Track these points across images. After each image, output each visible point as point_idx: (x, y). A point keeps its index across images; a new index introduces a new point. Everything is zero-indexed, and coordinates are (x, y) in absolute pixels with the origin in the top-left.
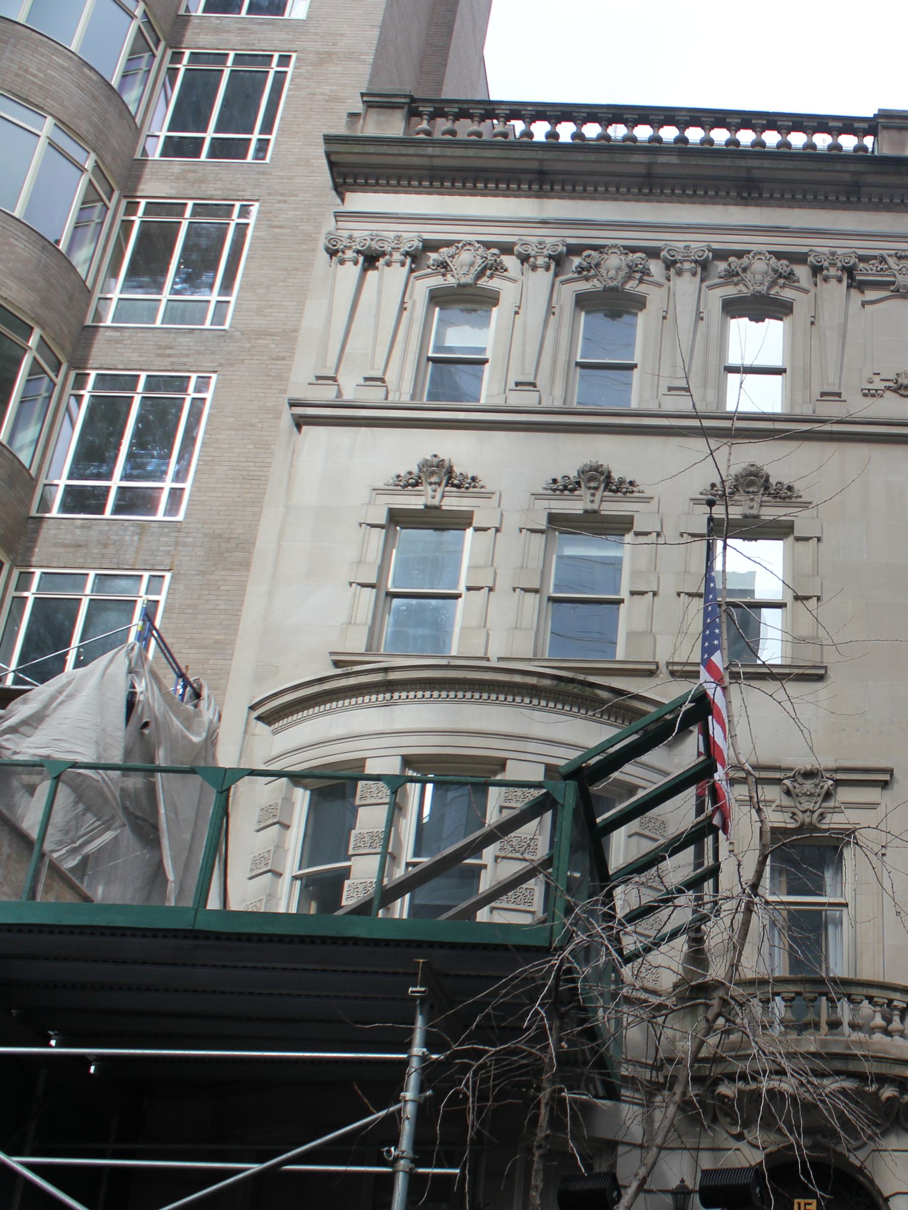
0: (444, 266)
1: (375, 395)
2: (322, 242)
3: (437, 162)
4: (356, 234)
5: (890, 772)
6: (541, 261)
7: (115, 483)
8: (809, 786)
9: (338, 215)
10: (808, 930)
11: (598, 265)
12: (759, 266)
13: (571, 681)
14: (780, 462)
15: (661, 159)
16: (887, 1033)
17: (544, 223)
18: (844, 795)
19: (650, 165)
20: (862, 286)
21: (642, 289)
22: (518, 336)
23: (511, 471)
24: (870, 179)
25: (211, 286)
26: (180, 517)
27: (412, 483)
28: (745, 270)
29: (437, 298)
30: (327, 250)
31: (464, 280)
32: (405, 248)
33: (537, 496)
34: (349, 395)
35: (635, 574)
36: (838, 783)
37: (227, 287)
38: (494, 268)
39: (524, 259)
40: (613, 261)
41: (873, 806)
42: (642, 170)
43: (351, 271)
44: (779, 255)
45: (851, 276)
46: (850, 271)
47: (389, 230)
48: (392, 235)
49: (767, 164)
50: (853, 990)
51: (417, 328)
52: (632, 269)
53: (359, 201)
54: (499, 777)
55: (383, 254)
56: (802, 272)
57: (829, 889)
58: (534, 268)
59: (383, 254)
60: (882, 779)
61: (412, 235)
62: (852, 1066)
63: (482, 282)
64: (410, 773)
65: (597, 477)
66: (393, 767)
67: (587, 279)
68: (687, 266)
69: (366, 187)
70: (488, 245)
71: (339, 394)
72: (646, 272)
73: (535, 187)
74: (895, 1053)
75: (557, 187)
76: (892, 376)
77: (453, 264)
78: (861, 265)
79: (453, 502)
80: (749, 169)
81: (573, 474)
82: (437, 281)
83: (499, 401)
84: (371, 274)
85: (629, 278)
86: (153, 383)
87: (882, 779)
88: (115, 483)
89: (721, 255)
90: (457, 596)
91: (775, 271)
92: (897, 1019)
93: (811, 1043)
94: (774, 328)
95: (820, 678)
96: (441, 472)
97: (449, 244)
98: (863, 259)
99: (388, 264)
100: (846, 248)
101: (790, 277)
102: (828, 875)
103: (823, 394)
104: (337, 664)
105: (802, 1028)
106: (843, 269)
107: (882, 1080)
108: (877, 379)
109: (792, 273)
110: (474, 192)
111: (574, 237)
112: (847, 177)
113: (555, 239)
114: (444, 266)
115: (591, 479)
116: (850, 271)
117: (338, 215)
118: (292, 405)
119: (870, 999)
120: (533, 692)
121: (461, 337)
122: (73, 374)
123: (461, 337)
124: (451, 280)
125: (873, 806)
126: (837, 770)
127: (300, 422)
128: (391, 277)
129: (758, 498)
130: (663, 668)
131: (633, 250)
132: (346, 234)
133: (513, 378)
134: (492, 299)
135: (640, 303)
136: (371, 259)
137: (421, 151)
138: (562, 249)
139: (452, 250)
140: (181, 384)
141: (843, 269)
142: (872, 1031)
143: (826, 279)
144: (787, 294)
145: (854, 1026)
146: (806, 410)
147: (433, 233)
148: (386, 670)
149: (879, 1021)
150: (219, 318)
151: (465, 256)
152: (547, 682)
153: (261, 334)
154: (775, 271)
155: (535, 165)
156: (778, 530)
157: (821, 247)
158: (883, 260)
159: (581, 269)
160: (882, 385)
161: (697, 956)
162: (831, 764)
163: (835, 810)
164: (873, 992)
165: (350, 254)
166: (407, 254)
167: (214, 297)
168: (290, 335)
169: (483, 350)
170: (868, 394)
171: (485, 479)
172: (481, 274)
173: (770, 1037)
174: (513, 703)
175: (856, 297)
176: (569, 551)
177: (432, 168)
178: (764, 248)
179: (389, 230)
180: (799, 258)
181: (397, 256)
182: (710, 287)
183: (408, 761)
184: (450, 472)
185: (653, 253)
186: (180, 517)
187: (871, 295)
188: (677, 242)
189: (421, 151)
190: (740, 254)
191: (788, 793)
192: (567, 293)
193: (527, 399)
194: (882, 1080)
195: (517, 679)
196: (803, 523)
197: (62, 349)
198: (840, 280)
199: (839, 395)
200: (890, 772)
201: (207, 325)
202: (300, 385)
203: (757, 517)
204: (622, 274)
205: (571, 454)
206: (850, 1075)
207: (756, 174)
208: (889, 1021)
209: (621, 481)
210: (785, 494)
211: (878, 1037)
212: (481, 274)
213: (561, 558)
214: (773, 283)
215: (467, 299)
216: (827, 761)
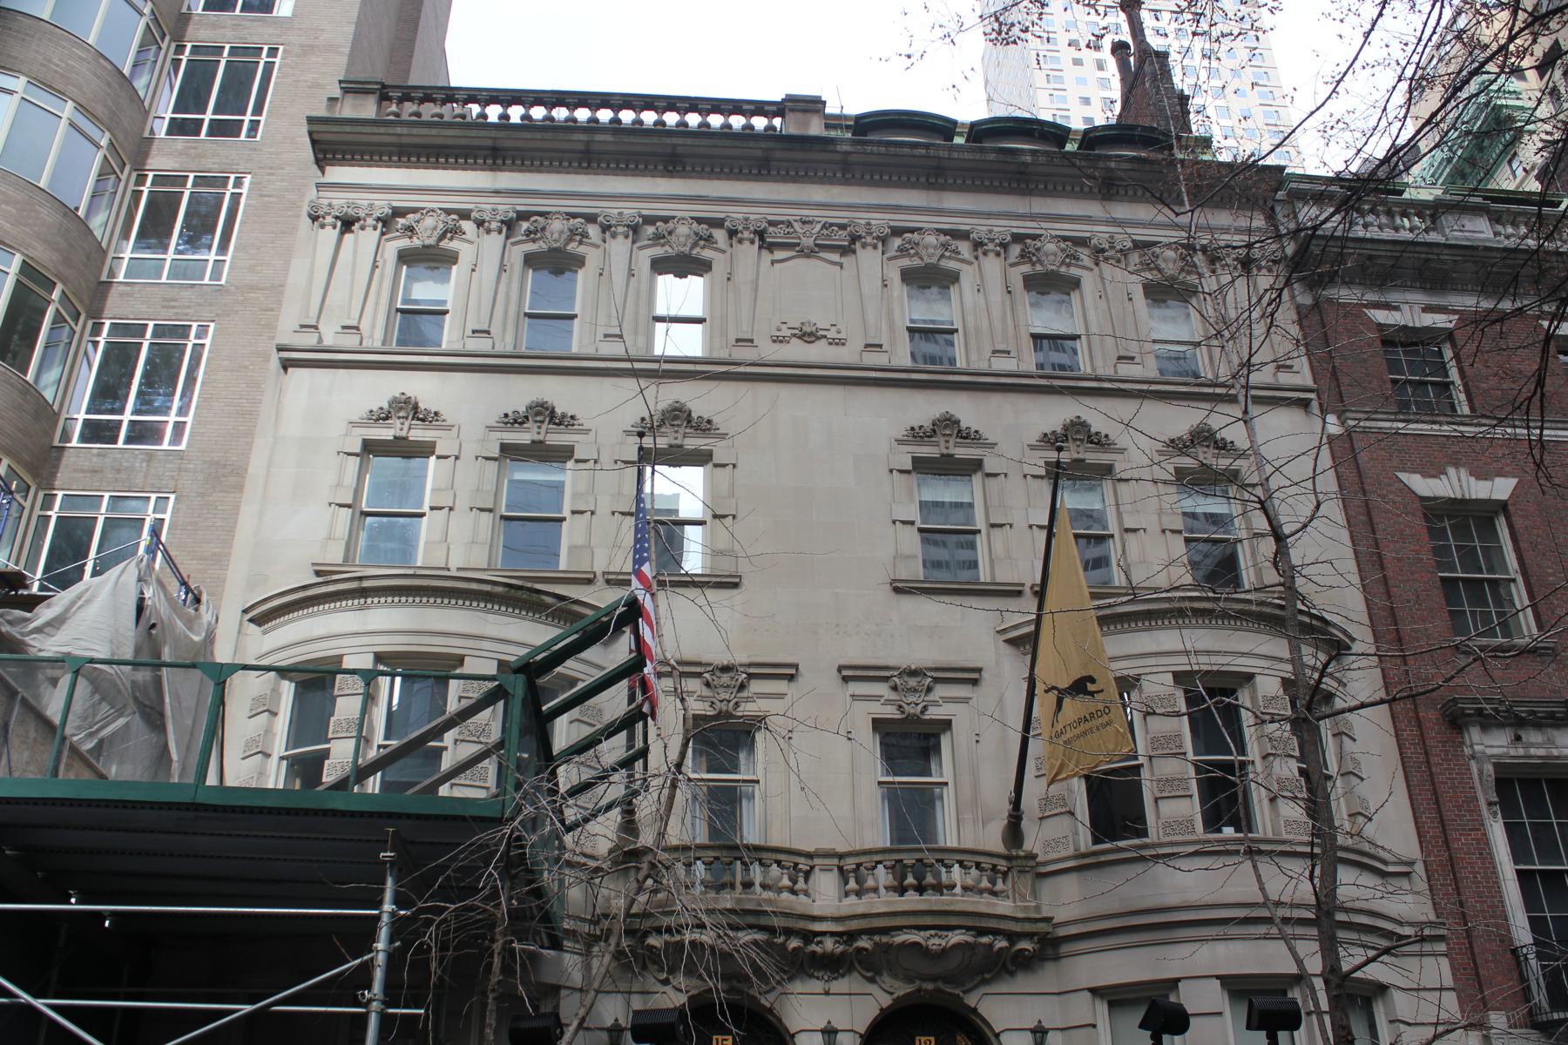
0: (410, 230)
1: (350, 341)
2: (306, 209)
3: (405, 140)
4: (335, 202)
5: (796, 666)
6: (494, 225)
7: (127, 417)
8: (725, 678)
9: (319, 186)
10: (725, 804)
11: (543, 229)
12: (683, 230)
13: (521, 588)
14: (700, 399)
15: (599, 137)
16: (793, 892)
17: (497, 192)
18: (756, 686)
19: (588, 143)
20: (771, 247)
21: (582, 249)
22: (475, 290)
23: (468, 407)
24: (779, 154)
25: (210, 247)
26: (183, 447)
27: (383, 417)
28: (670, 233)
29: (405, 257)
30: (310, 216)
31: (427, 242)
32: (377, 214)
33: (491, 428)
34: (328, 341)
35: (575, 495)
36: (751, 676)
37: (223, 248)
38: (455, 232)
39: (480, 224)
40: (557, 225)
41: (781, 696)
42: (581, 147)
43: (330, 234)
44: (700, 221)
45: (762, 239)
46: (761, 234)
47: (363, 199)
48: (366, 203)
49: (689, 141)
50: (764, 855)
51: (387, 284)
52: (573, 232)
53: (337, 174)
54: (458, 671)
55: (358, 219)
56: (720, 235)
57: (743, 768)
58: (488, 231)
59: (358, 219)
60: (788, 673)
61: (383, 203)
62: (763, 921)
63: (443, 244)
64: (381, 668)
65: (543, 412)
66: (366, 662)
67: (534, 241)
68: (620, 229)
69: (343, 162)
70: (448, 212)
71: (320, 340)
72: (585, 235)
73: (489, 161)
74: (800, 910)
75: (508, 162)
76: (797, 325)
77: (419, 228)
78: (771, 229)
79: (418, 434)
80: (674, 146)
81: (522, 409)
82: (404, 243)
83: (458, 347)
84: (347, 236)
85: (571, 240)
86: (159, 331)
87: (788, 673)
88: (127, 417)
89: (650, 220)
90: (422, 515)
91: (696, 234)
92: (801, 880)
93: (727, 900)
94: (695, 284)
95: (735, 586)
96: (408, 408)
97: (414, 210)
98: (772, 223)
99: (363, 228)
100: (757, 214)
101: (709, 239)
102: (742, 756)
103: (738, 340)
104: (318, 573)
105: (720, 888)
106: (755, 232)
107: (789, 932)
108: (784, 327)
109: (711, 236)
110: (436, 166)
111: (523, 204)
112: (759, 153)
113: (506, 207)
114: (410, 230)
115: (538, 414)
116: (761, 234)
117: (319, 186)
118: (280, 349)
119: (779, 863)
120: (488, 597)
121: (426, 291)
122: (90, 323)
123: (426, 291)
124: (416, 242)
125: (781, 696)
126: (750, 665)
127: (286, 365)
128: (365, 240)
129: (682, 430)
130: (600, 577)
131: (574, 216)
132: (326, 202)
133: (470, 326)
134: (452, 258)
135: (580, 261)
136: (347, 224)
137: (391, 131)
138: (512, 215)
139: (418, 216)
140: (183, 331)
141: (755, 232)
142: (780, 890)
143: (740, 241)
144: (707, 254)
145: (764, 886)
146: (723, 354)
147: (401, 201)
148: (360, 579)
149: (786, 882)
150: (216, 274)
151: (429, 222)
152: (499, 589)
153: (253, 288)
154: (696, 234)
155: (489, 143)
156: (700, 458)
157: (736, 213)
158: (789, 224)
159: (528, 233)
161: (629, 826)
162: (745, 660)
163: (748, 700)
164: (781, 857)
165: (329, 219)
166: (378, 219)
167: (212, 256)
168: (278, 289)
169: (444, 302)
170: (777, 340)
171: (445, 414)
172: (442, 237)
173: (692, 895)
175: (767, 257)
176: (518, 476)
177: (401, 145)
178: (687, 214)
179: (363, 199)
180: (717, 223)
181: (370, 221)
182: (641, 248)
183: (379, 658)
184: (416, 407)
185: (591, 219)
186: (183, 447)
187: (779, 255)
188: (612, 209)
189: (391, 131)
190: (666, 220)
191: (708, 685)
192: (517, 254)
193: (482, 344)
194: (789, 932)
195: (474, 586)
196: (721, 453)
197: (81, 301)
198: (752, 242)
199: (751, 341)
200: (796, 666)
201: (206, 281)
202: (287, 333)
203: (681, 446)
204: (564, 236)
205: (520, 392)
206: (761, 928)
207: (680, 150)
208: (795, 882)
209: (564, 416)
210: (704, 427)
211: (785, 895)
212: (442, 237)
213: (510, 481)
214: (695, 245)
215: (433, 258)
216: (741, 657)
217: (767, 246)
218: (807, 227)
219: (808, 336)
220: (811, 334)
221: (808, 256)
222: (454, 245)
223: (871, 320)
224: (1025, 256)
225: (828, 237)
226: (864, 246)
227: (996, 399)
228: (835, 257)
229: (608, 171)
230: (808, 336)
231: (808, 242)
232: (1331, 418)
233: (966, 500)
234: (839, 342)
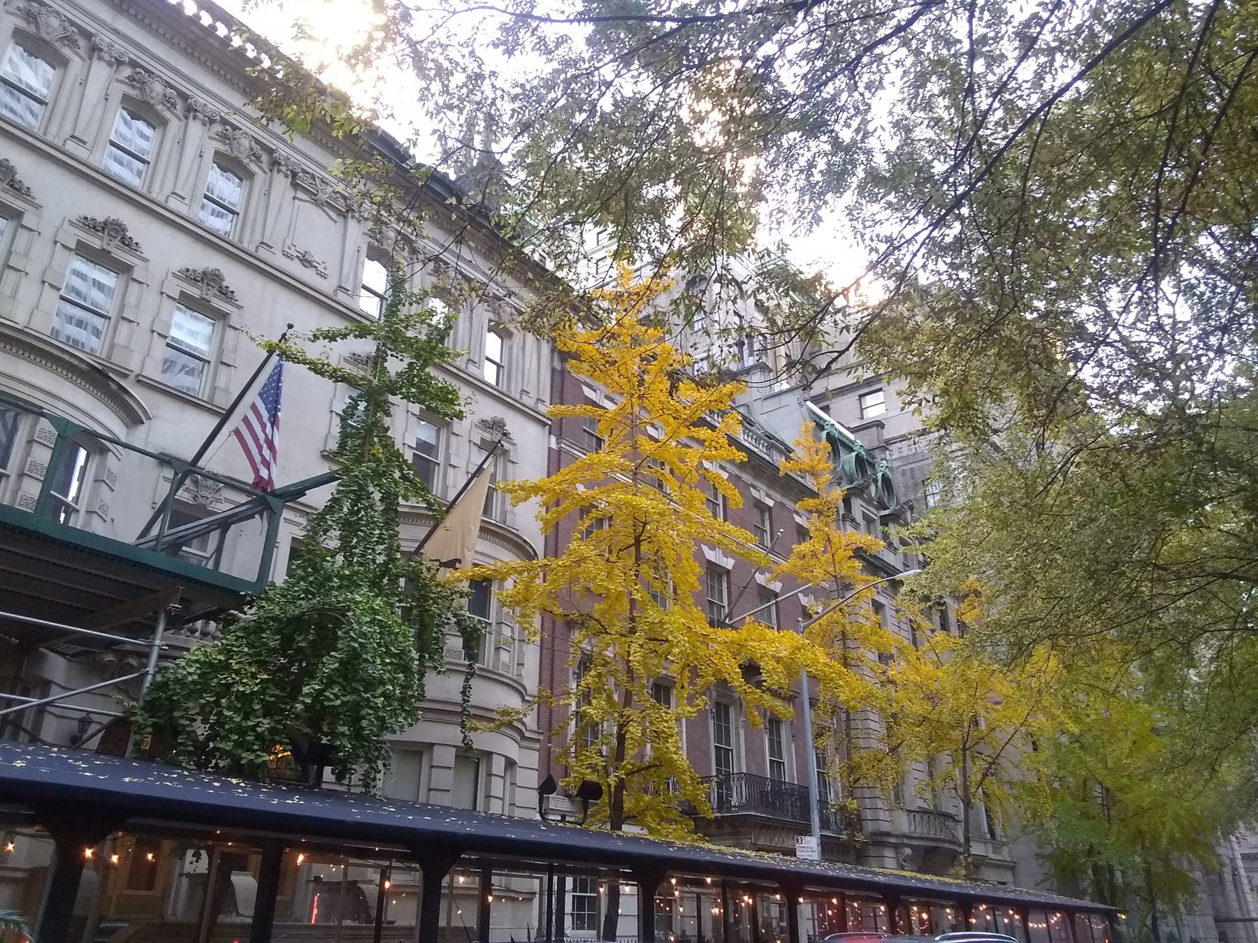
12: (246, 142)
21: (167, 114)
31: (48, 38)
38: (68, 40)
46: (294, 175)
52: (166, 100)
63: (58, 45)
67: (133, 87)
70: (72, 23)
72: (174, 105)
81: (100, 219)
82: (22, 24)
89: (224, 122)
98: (304, 171)
101: (258, 158)
115: (114, 230)
116: (294, 175)
131: (172, 87)
139: (43, 10)
152: (84, 366)
154: (252, 149)
158: (313, 177)
159: (131, 79)
160: (296, 254)
174: (55, 372)
175: (291, 193)
187: (300, 195)
188: (200, 99)
190: (235, 128)
192: (119, 90)
195: (66, 357)
205: (104, 208)
217: (295, 186)
218: (324, 186)
219: (306, 261)
220: (310, 262)
221: (317, 205)
222: (67, 52)
223: (346, 270)
224: (437, 271)
225: (335, 200)
226: (353, 217)
227: (273, 289)
228: (334, 215)
229: (203, 64)
230: (306, 261)
231: (324, 197)
232: (553, 439)
233: (432, 441)
234: (324, 276)
